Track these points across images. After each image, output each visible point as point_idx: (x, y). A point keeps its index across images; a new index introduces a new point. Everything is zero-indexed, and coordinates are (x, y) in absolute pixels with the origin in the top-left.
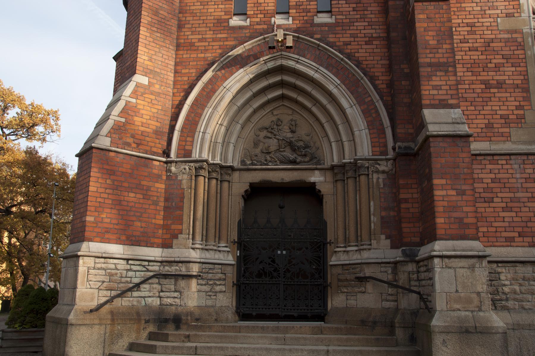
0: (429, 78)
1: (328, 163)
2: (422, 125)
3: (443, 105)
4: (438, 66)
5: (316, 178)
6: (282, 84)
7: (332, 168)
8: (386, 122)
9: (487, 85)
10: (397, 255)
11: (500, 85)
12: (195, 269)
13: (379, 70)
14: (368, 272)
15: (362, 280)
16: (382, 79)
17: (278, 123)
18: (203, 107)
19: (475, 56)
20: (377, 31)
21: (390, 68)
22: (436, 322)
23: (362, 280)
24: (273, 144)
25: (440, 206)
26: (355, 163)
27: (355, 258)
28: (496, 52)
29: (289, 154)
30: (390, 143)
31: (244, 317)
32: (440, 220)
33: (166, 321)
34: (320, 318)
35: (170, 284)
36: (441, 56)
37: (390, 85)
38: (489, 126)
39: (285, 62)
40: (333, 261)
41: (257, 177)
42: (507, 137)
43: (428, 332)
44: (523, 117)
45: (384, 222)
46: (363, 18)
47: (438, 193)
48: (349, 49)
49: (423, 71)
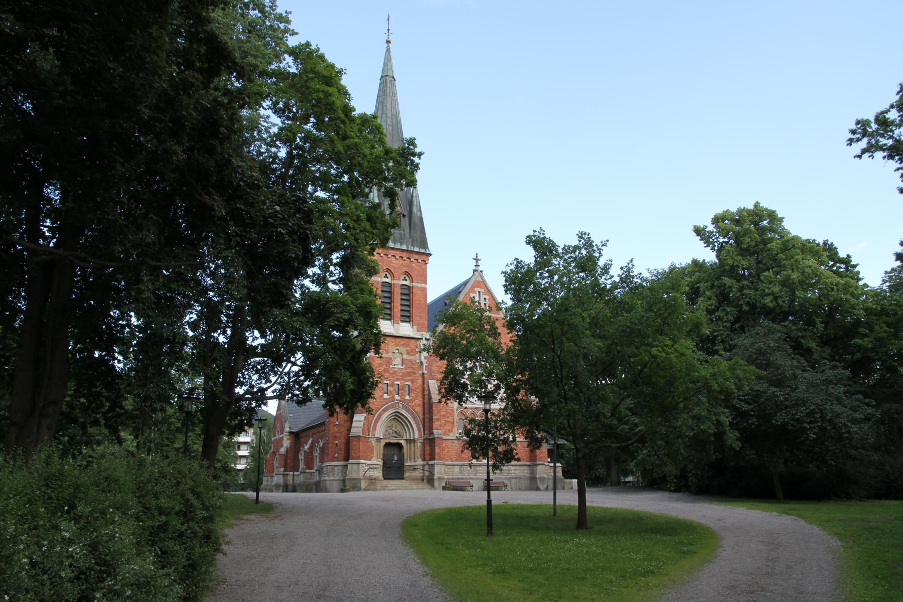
0: (435, 422)
1: (405, 438)
2: (433, 433)
3: (437, 429)
4: (438, 420)
5: (402, 442)
6: (394, 415)
7: (406, 440)
8: (422, 429)
9: (446, 421)
10: (422, 463)
11: (448, 421)
12: (377, 466)
13: (421, 415)
14: (416, 467)
15: (415, 469)
16: (422, 417)
17: (392, 425)
18: (378, 422)
19: (443, 413)
20: (421, 403)
21: (424, 414)
22: (435, 477)
23: (415, 469)
24: (391, 431)
25: (436, 452)
26: (414, 440)
27: (413, 464)
28: (448, 413)
29: (395, 434)
30: (423, 435)
31: (385, 479)
32: (436, 456)
33: (372, 479)
34: (403, 479)
35: (372, 470)
36: (438, 417)
37: (424, 419)
38: (445, 432)
39: (399, 411)
40: (406, 464)
41: (387, 441)
42: (449, 435)
43: (433, 479)
44: (452, 430)
45: (421, 455)
46: (417, 399)
47: (436, 450)
48: (414, 408)
49: (434, 420)
